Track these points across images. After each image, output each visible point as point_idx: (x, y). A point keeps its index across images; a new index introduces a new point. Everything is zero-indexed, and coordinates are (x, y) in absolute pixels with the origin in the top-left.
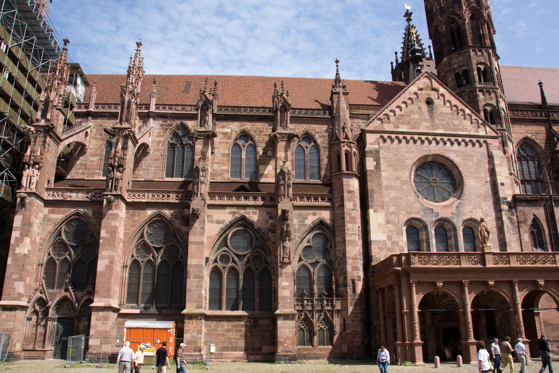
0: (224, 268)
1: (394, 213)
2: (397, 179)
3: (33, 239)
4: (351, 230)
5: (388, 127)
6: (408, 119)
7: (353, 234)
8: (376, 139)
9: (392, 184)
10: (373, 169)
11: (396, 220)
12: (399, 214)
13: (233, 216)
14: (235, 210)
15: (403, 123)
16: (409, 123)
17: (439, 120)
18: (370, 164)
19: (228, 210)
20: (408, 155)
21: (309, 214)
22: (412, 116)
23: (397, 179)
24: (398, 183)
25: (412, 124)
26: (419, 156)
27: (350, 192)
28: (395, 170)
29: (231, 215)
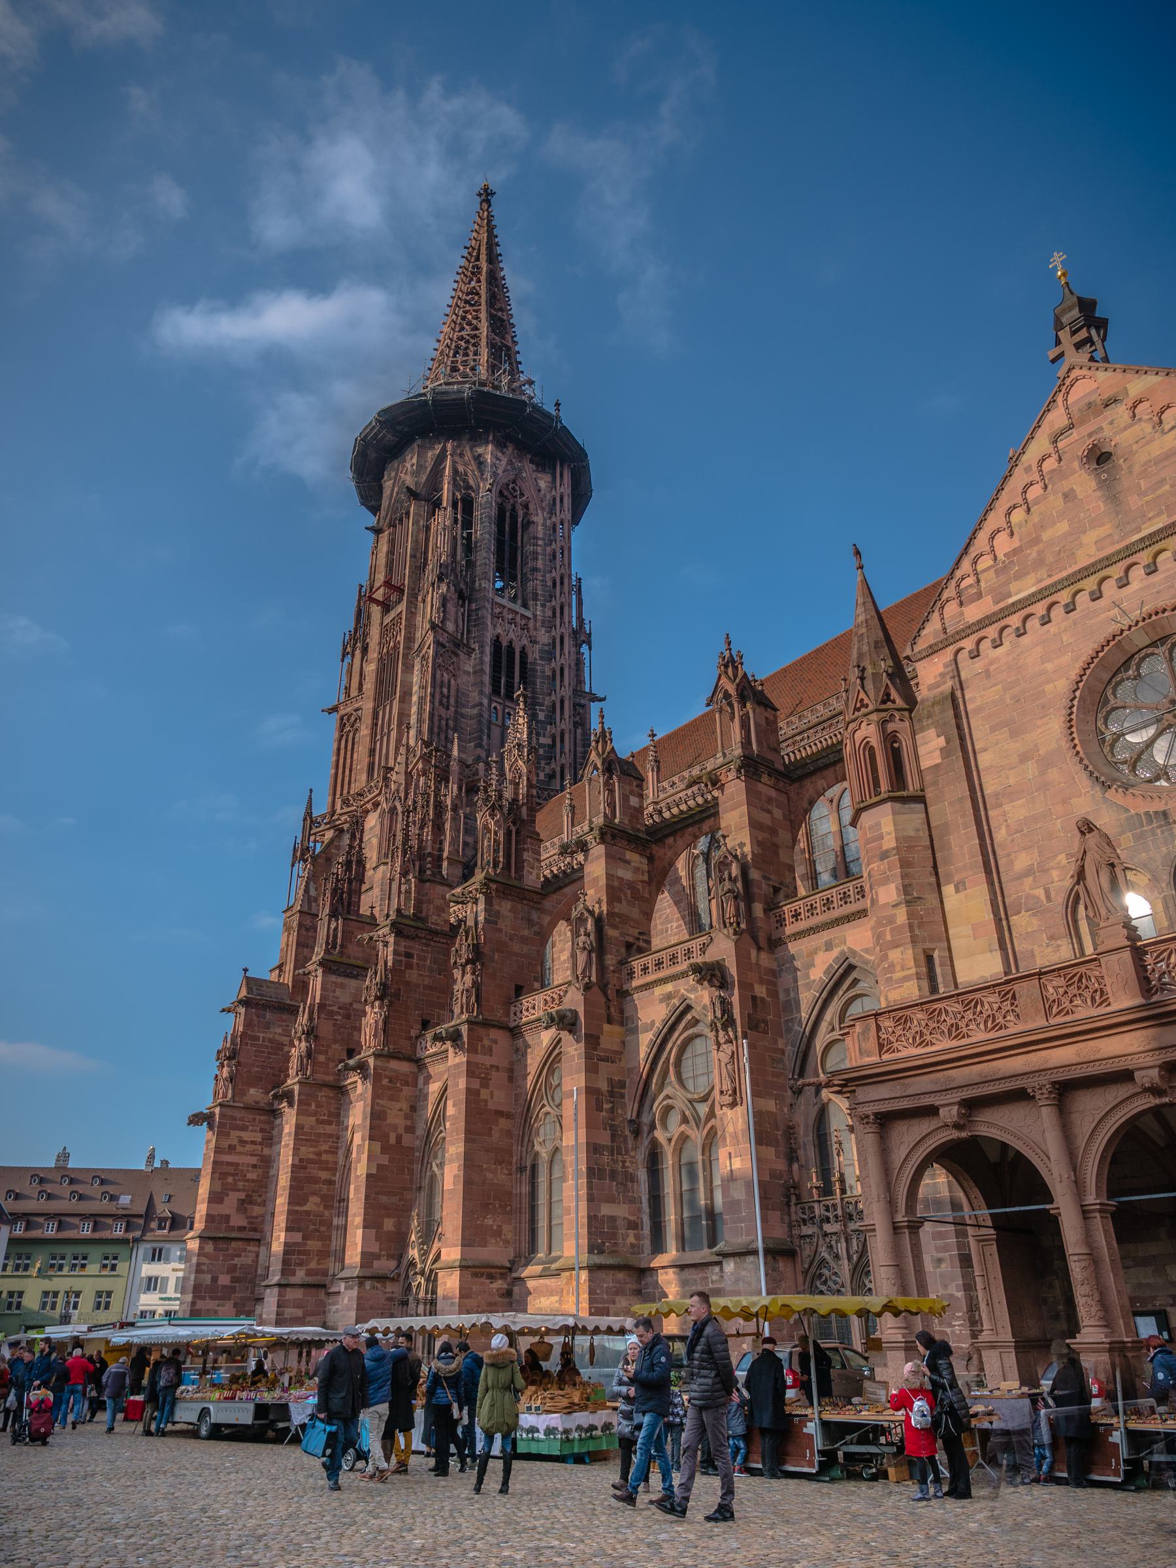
0: (670, 1140)
1: (1029, 872)
2: (1024, 758)
3: (393, 1141)
4: (898, 968)
5: (973, 613)
6: (1033, 553)
7: (906, 979)
8: (945, 666)
9: (1012, 781)
10: (939, 761)
11: (1040, 893)
12: (1045, 871)
13: (668, 1005)
14: (669, 987)
15: (1018, 576)
16: (1040, 562)
17: (1142, 494)
18: (930, 748)
19: (659, 991)
20: (1049, 666)
21: (815, 952)
22: (1046, 536)
23: (1024, 758)
24: (1031, 768)
25: (1050, 559)
26: (1087, 649)
27: (884, 855)
28: (1014, 735)
29: (664, 1005)
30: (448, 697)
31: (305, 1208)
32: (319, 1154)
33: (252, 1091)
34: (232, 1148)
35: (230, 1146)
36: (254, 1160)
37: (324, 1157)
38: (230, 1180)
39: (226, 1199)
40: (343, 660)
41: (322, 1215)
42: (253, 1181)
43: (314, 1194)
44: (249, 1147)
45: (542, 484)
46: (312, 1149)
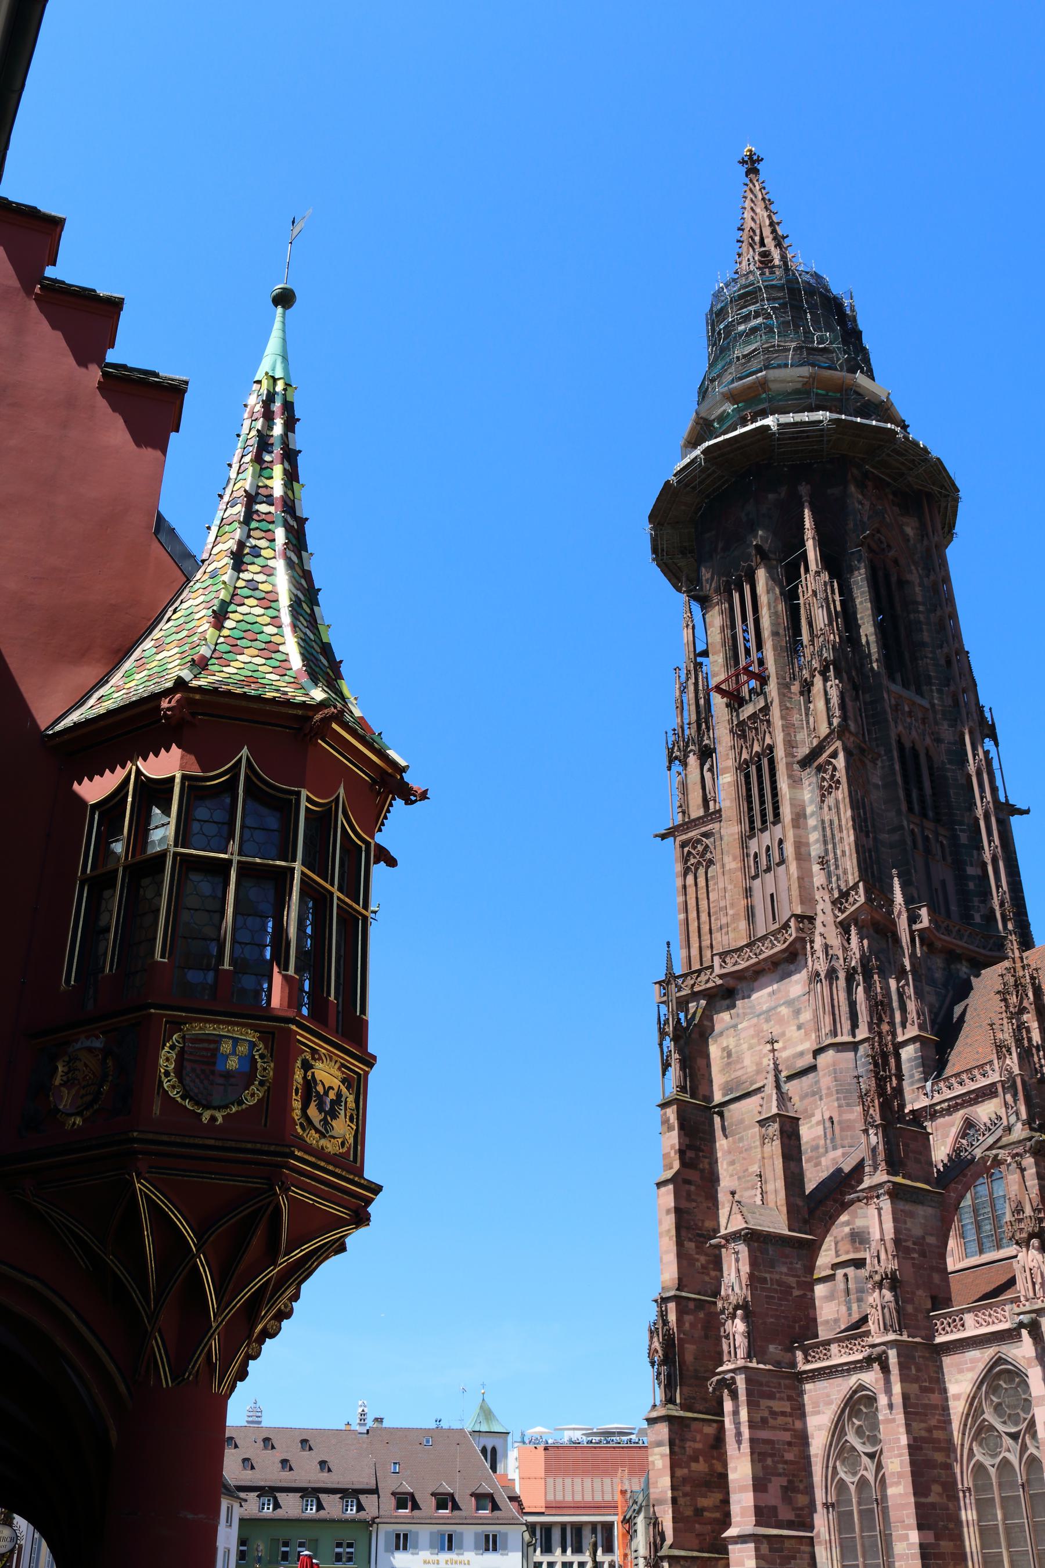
30: (865, 821)
31: (930, 1500)
32: (929, 1430)
33: (772, 1348)
34: (764, 1421)
35: (762, 1418)
36: (787, 1436)
37: (937, 1434)
38: (769, 1461)
39: (770, 1485)
40: (669, 769)
41: (948, 1509)
42: (791, 1462)
43: (935, 1481)
44: (781, 1420)
45: (909, 531)
46: (923, 1425)
